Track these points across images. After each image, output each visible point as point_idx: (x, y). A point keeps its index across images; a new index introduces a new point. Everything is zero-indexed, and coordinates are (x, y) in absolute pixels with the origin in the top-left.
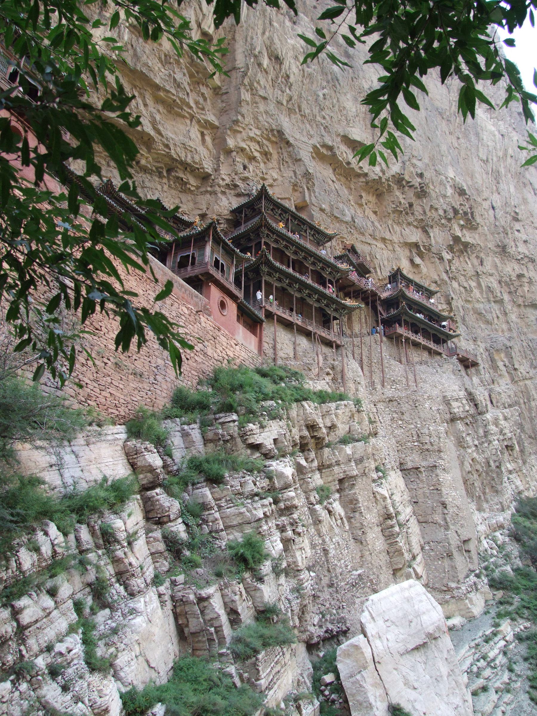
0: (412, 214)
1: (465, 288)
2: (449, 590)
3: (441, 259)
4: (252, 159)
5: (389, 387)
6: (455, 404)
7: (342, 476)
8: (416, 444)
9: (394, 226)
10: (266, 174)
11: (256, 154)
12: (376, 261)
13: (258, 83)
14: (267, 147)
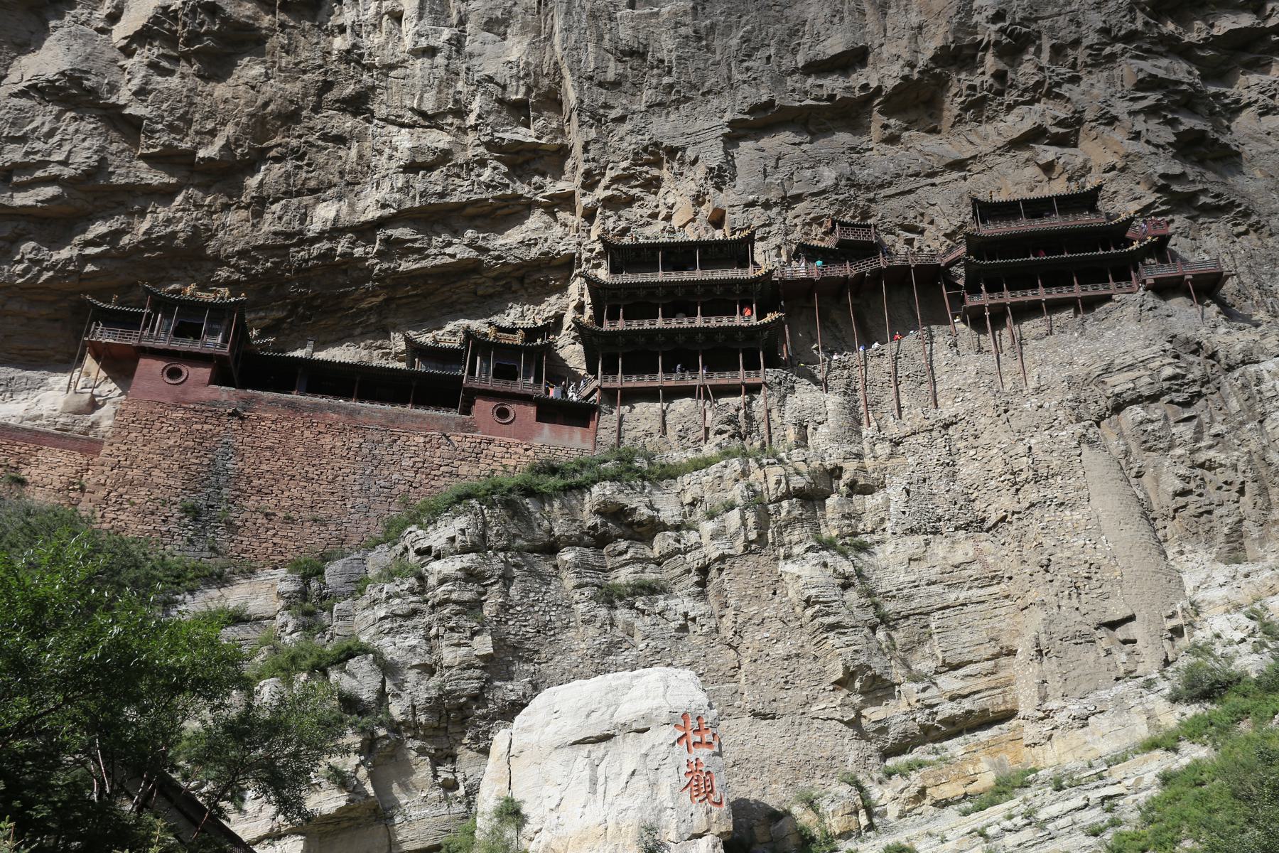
5: (949, 403)
8: (1002, 478)
10: (657, 206)
11: (633, 192)
14: (647, 173)
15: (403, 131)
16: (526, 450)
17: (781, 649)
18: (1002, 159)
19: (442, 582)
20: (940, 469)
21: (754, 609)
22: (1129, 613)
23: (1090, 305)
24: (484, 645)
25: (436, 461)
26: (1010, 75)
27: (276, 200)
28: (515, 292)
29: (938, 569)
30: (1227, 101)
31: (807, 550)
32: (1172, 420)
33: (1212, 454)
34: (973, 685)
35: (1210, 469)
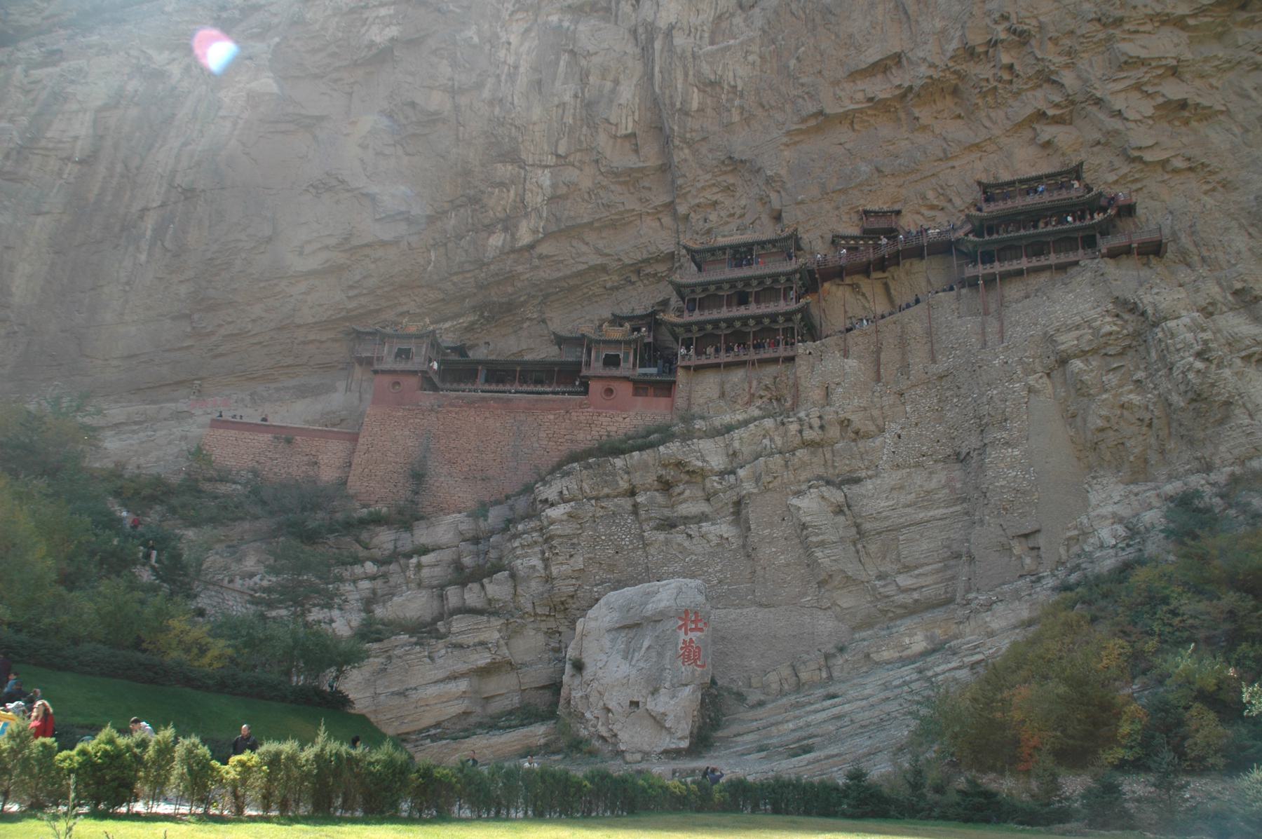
0: (1017, 76)
2: (968, 602)
3: (1098, 102)
4: (715, 203)
6: (1061, 338)
7: (735, 498)
9: (993, 115)
11: (715, 198)
12: (948, 192)
13: (692, 130)
17: (782, 559)
20: (928, 414)
21: (767, 532)
22: (1037, 527)
23: (1062, 268)
24: (579, 562)
25: (563, 432)
26: (1017, 67)
27: (463, 237)
28: (633, 283)
29: (913, 495)
31: (810, 487)
33: (1132, 396)
34: (922, 581)
35: (1126, 409)
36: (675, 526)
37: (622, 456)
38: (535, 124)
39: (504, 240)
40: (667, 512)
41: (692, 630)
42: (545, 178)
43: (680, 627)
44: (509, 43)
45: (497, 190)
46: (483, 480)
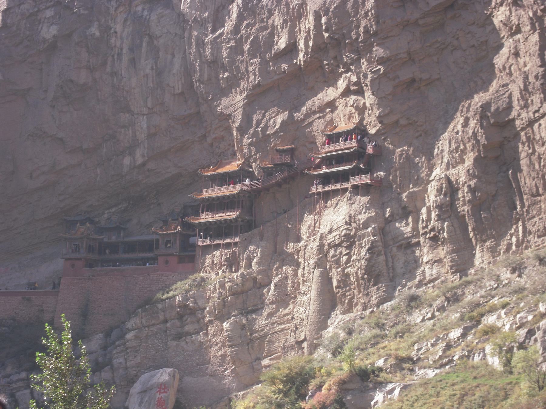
1: (473, 46)
4: (223, 138)
11: (222, 134)
15: (145, 117)
16: (173, 277)
18: (342, 101)
19: (128, 341)
21: (214, 340)
24: (138, 359)
26: (338, 58)
30: (438, 45)
32: (343, 254)
33: (349, 269)
36: (181, 338)
37: (162, 303)
38: (134, 89)
39: (130, 161)
40: (180, 330)
41: (162, 393)
42: (143, 122)
43: (157, 392)
44: (116, 32)
45: (123, 130)
46: (111, 315)
